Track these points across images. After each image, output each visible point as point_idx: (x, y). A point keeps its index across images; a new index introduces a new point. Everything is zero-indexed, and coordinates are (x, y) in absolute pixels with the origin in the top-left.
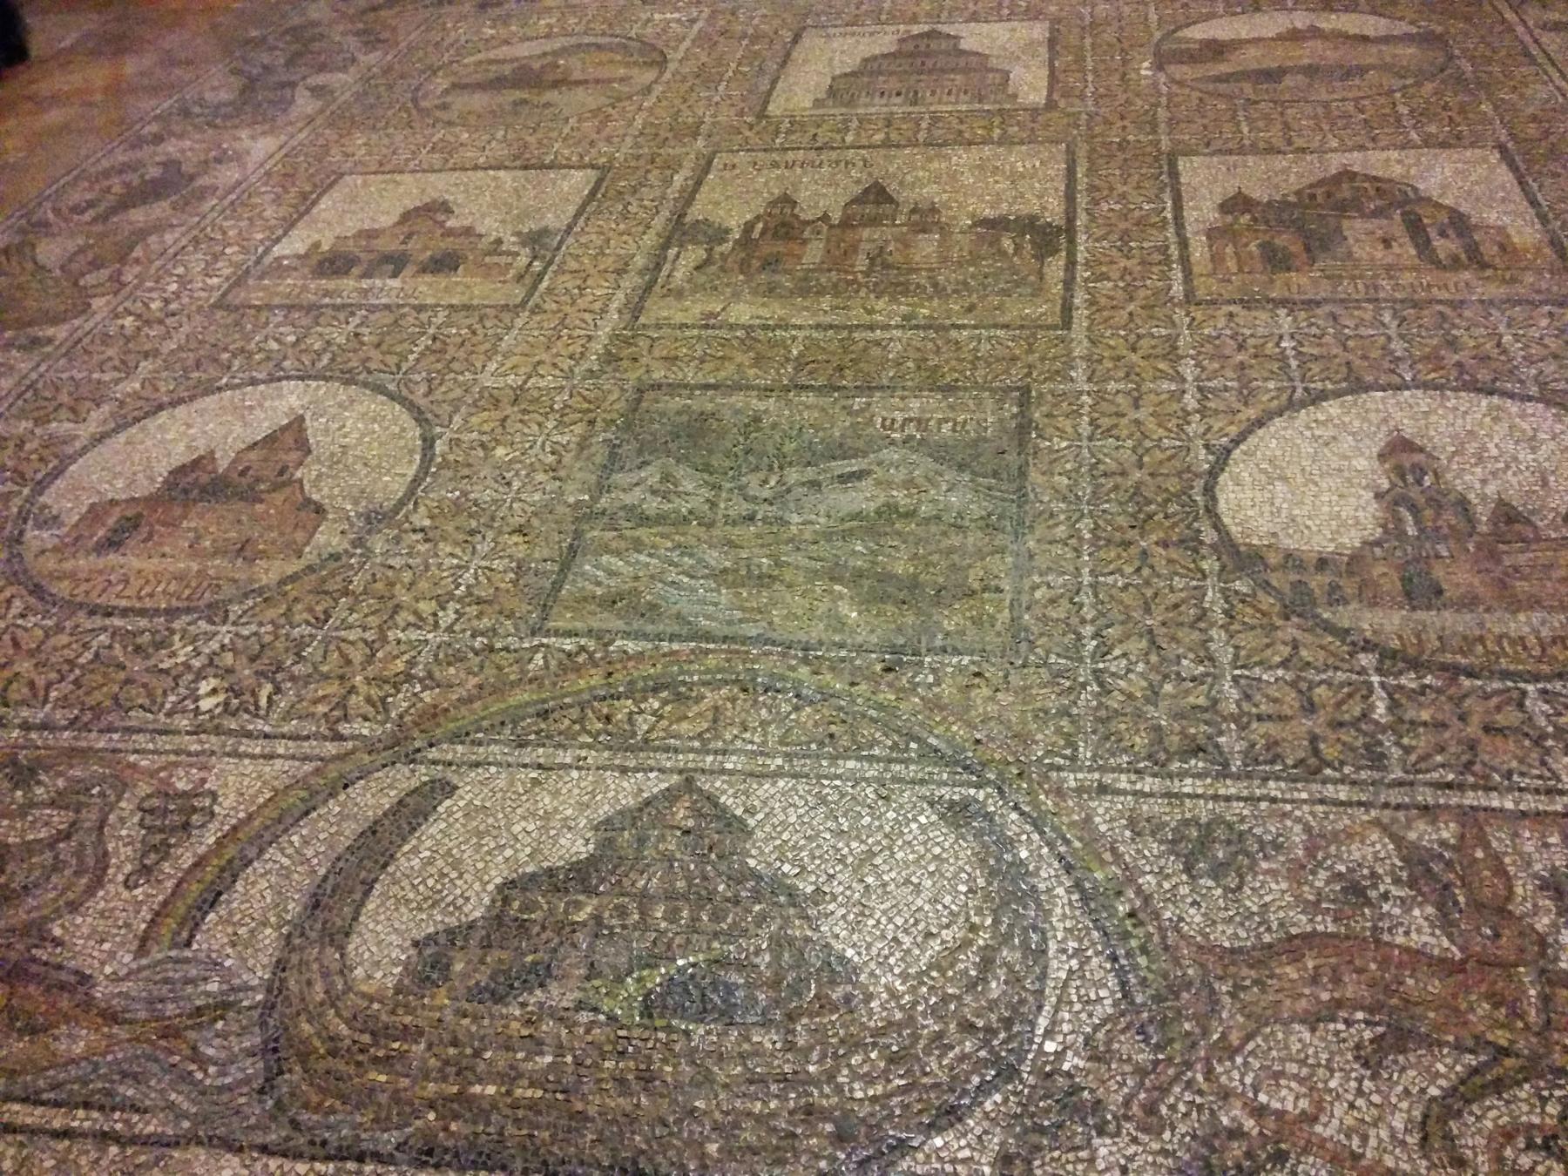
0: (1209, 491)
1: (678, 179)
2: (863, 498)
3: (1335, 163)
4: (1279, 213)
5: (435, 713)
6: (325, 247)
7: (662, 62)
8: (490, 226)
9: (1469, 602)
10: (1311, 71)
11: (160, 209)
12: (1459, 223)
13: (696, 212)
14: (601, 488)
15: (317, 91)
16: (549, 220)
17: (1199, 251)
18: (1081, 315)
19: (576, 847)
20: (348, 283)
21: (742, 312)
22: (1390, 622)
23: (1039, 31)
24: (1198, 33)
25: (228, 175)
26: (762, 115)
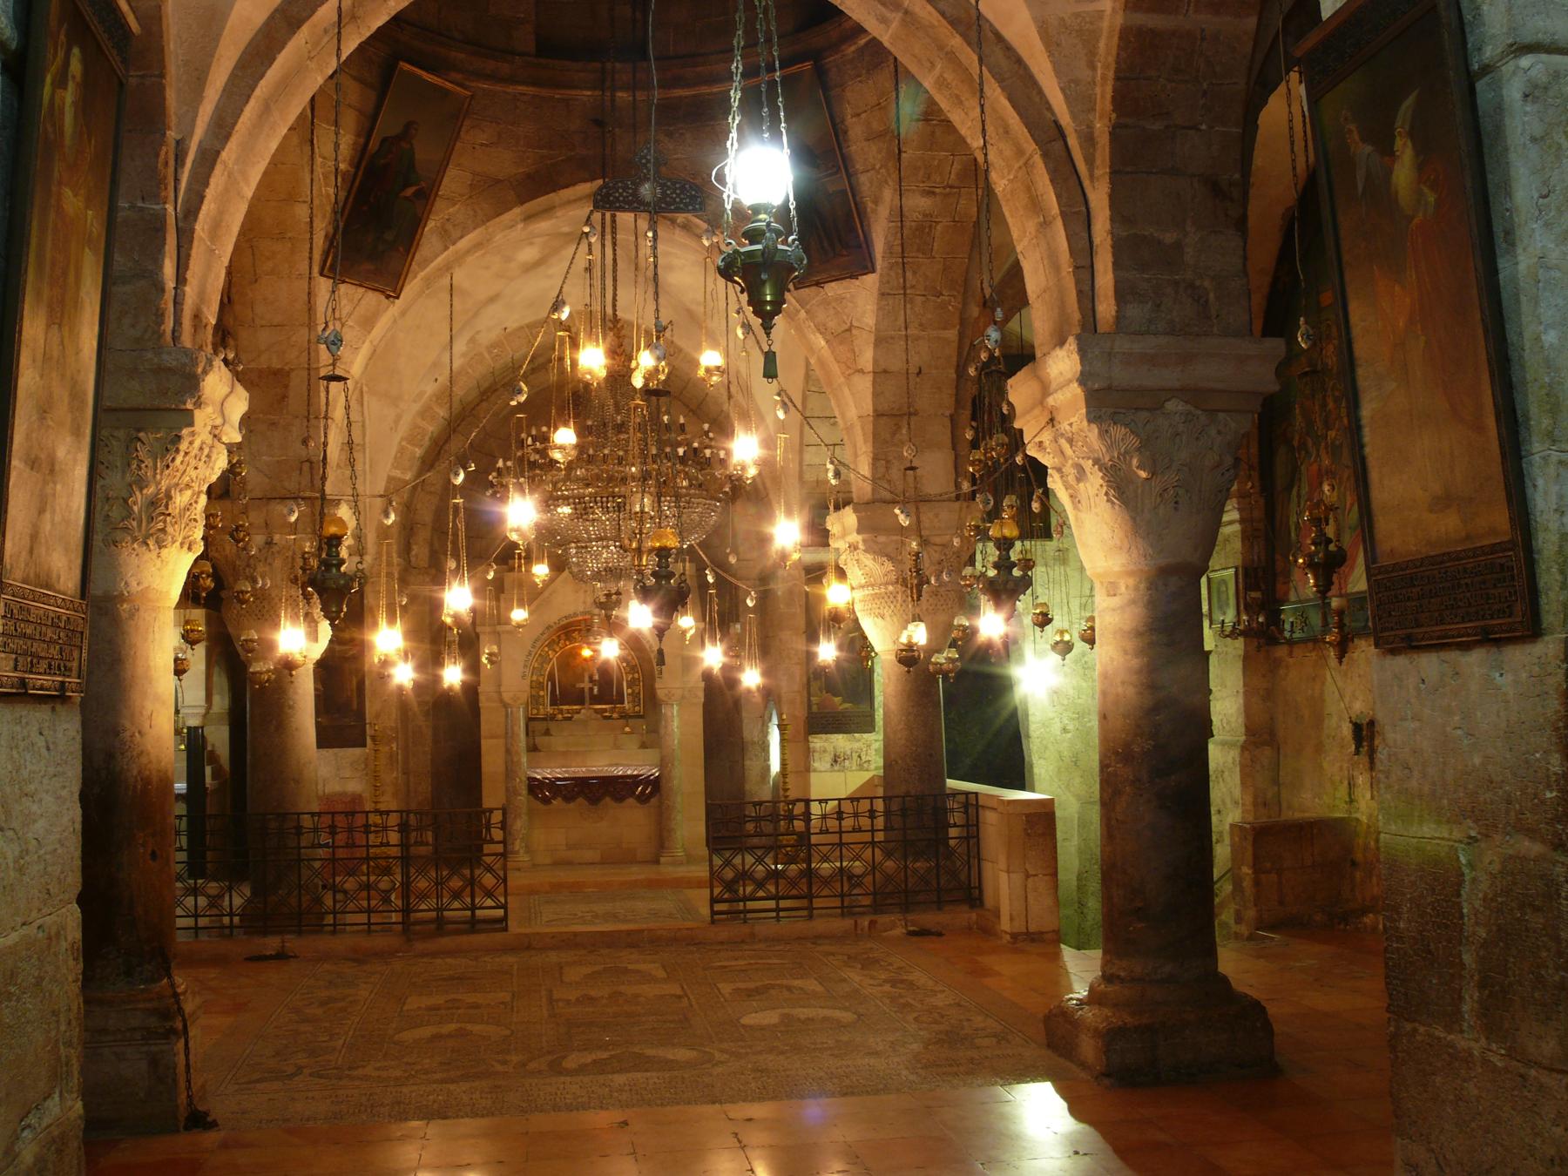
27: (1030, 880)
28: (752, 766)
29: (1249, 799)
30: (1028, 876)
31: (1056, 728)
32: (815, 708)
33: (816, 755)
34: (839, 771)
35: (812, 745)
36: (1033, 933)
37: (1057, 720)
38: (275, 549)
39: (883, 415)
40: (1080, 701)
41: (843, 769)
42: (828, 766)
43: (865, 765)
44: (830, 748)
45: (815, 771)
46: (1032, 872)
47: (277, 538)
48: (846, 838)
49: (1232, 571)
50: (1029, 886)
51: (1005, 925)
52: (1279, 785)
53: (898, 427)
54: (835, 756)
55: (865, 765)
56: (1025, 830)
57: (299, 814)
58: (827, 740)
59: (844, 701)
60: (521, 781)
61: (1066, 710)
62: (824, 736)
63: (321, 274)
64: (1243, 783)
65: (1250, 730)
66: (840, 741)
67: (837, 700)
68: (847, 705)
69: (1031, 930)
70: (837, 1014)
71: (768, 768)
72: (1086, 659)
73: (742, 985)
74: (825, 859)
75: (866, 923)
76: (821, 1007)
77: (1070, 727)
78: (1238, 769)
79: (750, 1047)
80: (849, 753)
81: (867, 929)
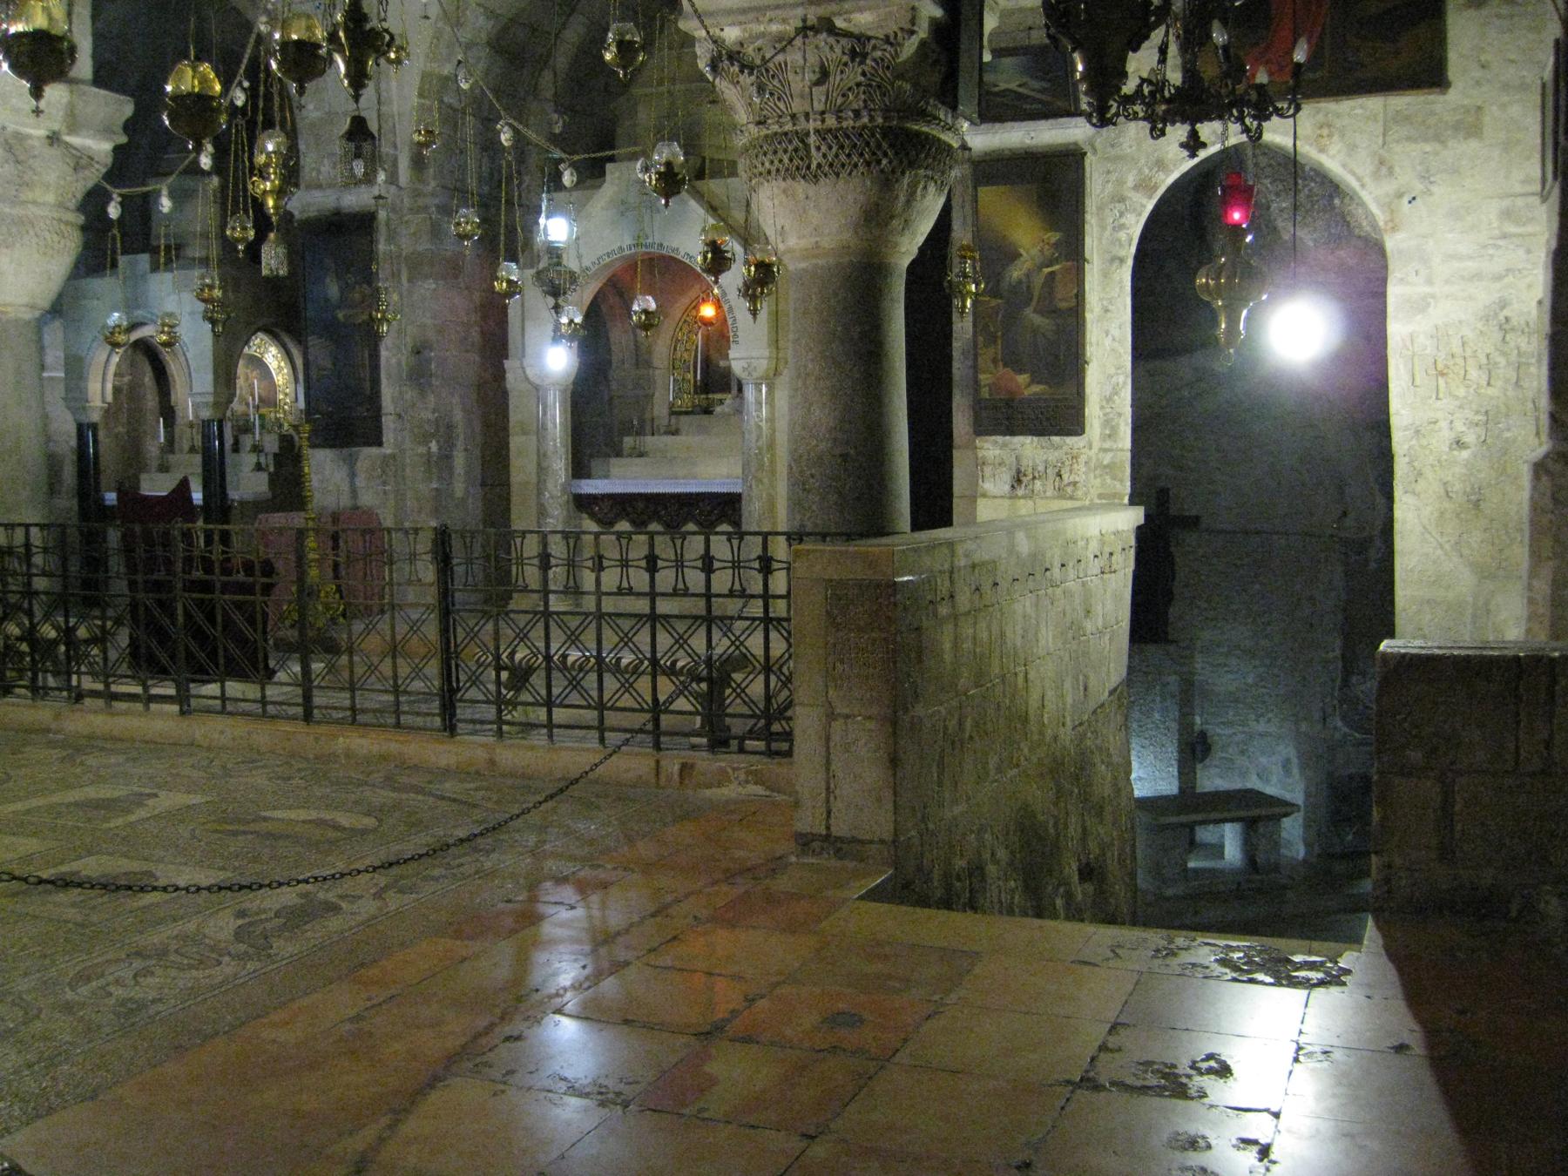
27: (837, 726)
30: (831, 716)
32: (985, 393)
33: (988, 470)
34: (1024, 497)
35: (980, 454)
36: (838, 839)
37: (1443, 424)
40: (1491, 391)
41: (1031, 495)
42: (1007, 488)
43: (1069, 490)
45: (984, 495)
46: (841, 709)
48: (664, 607)
50: (836, 738)
54: (1019, 472)
55: (1069, 490)
58: (1004, 445)
59: (1033, 381)
60: (552, 497)
61: (1460, 407)
62: (1000, 439)
66: (1028, 448)
67: (1022, 379)
68: (1036, 388)
69: (840, 828)
72: (1506, 312)
77: (1470, 438)
80: (1041, 468)
81: (676, 777)
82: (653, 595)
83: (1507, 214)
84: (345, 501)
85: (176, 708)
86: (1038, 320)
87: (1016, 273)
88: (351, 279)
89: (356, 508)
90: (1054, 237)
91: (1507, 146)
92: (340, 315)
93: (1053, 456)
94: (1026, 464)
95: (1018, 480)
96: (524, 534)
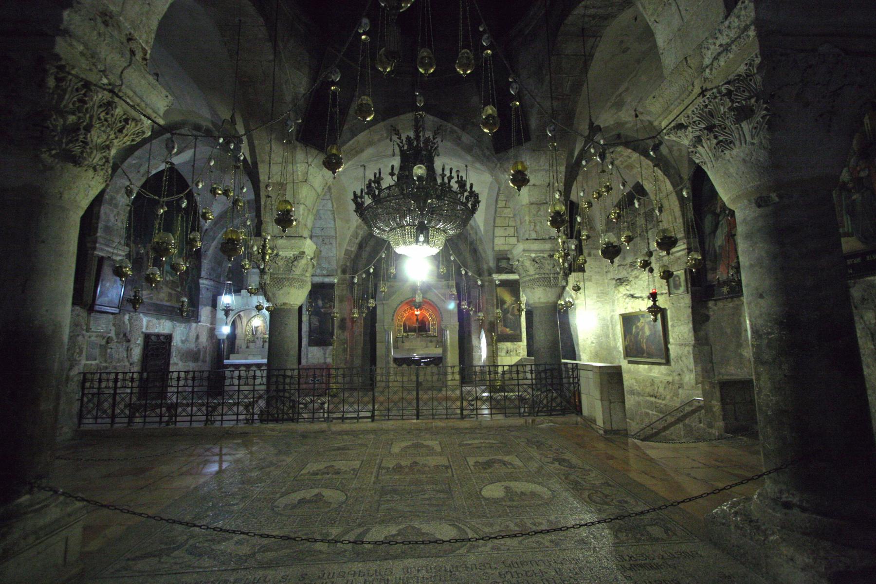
0: (480, 493)
1: (377, 462)
2: (427, 496)
3: (491, 458)
4: (483, 463)
5: (362, 523)
6: (311, 471)
7: (367, 447)
8: (344, 469)
9: (518, 501)
10: (485, 447)
11: (272, 468)
12: (510, 464)
13: (383, 465)
14: (381, 497)
15: (296, 452)
16: (355, 467)
17: (472, 468)
18: (455, 476)
19: (394, 532)
20: (319, 477)
21: (397, 477)
22: (509, 504)
23: (437, 442)
24: (465, 442)
25: (285, 463)
26: (390, 452)
27: (612, 405)
28: (475, 355)
29: (699, 369)
30: (611, 403)
31: (589, 342)
38: (280, 257)
39: (532, 204)
41: (510, 356)
44: (505, 347)
47: (280, 253)
48: (521, 382)
49: (683, 271)
51: (600, 422)
52: (713, 363)
53: (539, 210)
56: (608, 381)
57: (285, 370)
59: (511, 329)
63: (297, 139)
64: (695, 362)
65: (697, 338)
66: (509, 345)
67: (508, 330)
69: (615, 427)
70: (538, 489)
71: (481, 356)
73: (481, 459)
74: (513, 391)
75: (531, 421)
76: (526, 481)
78: (692, 356)
79: (491, 525)
82: (518, 380)
83: (598, 297)
84: (322, 361)
85: (370, 420)
86: (511, 317)
87: (506, 306)
88: (326, 301)
89: (325, 363)
90: (514, 299)
91: (597, 283)
92: (322, 310)
93: (515, 347)
94: (509, 349)
95: (507, 352)
96: (173, 372)
